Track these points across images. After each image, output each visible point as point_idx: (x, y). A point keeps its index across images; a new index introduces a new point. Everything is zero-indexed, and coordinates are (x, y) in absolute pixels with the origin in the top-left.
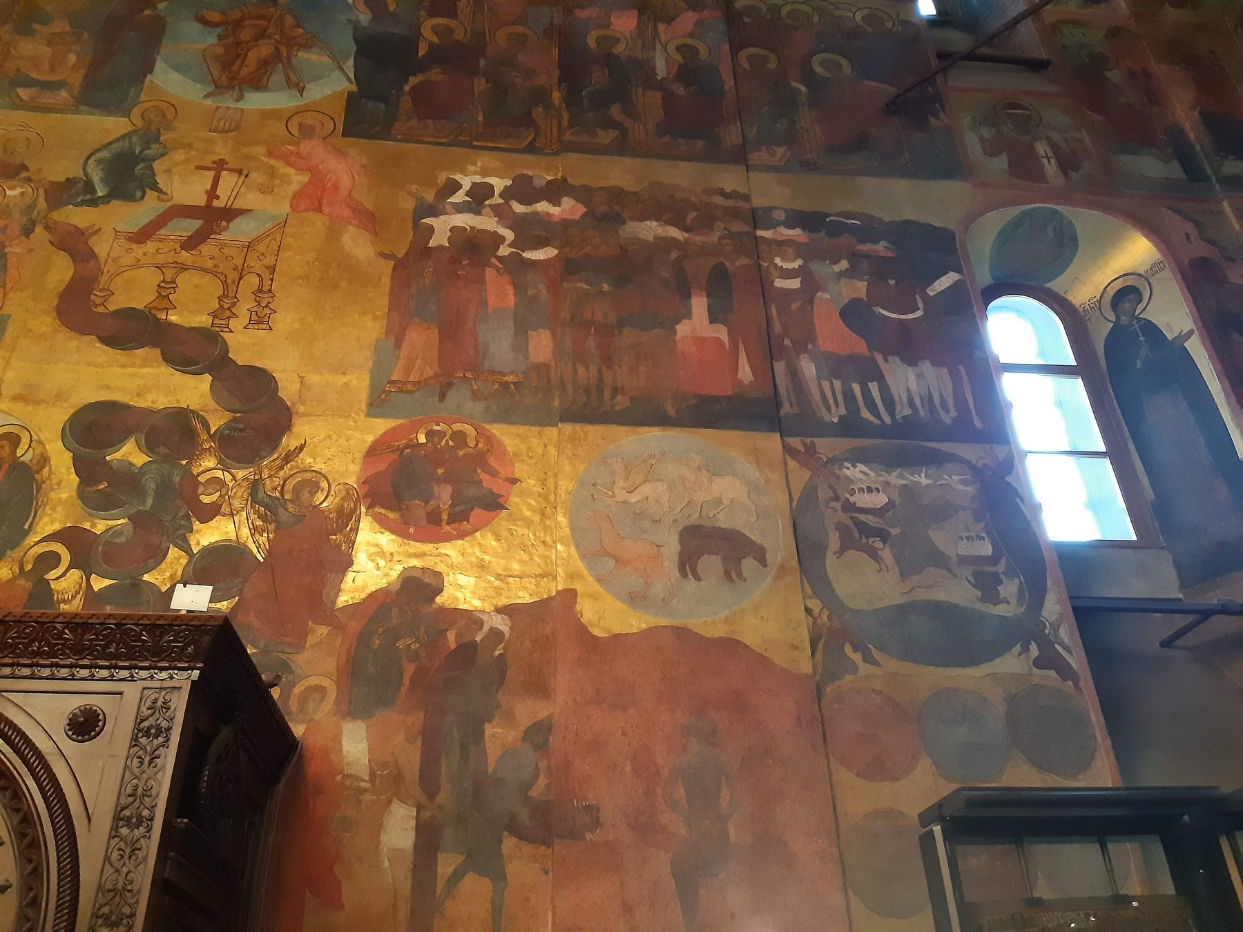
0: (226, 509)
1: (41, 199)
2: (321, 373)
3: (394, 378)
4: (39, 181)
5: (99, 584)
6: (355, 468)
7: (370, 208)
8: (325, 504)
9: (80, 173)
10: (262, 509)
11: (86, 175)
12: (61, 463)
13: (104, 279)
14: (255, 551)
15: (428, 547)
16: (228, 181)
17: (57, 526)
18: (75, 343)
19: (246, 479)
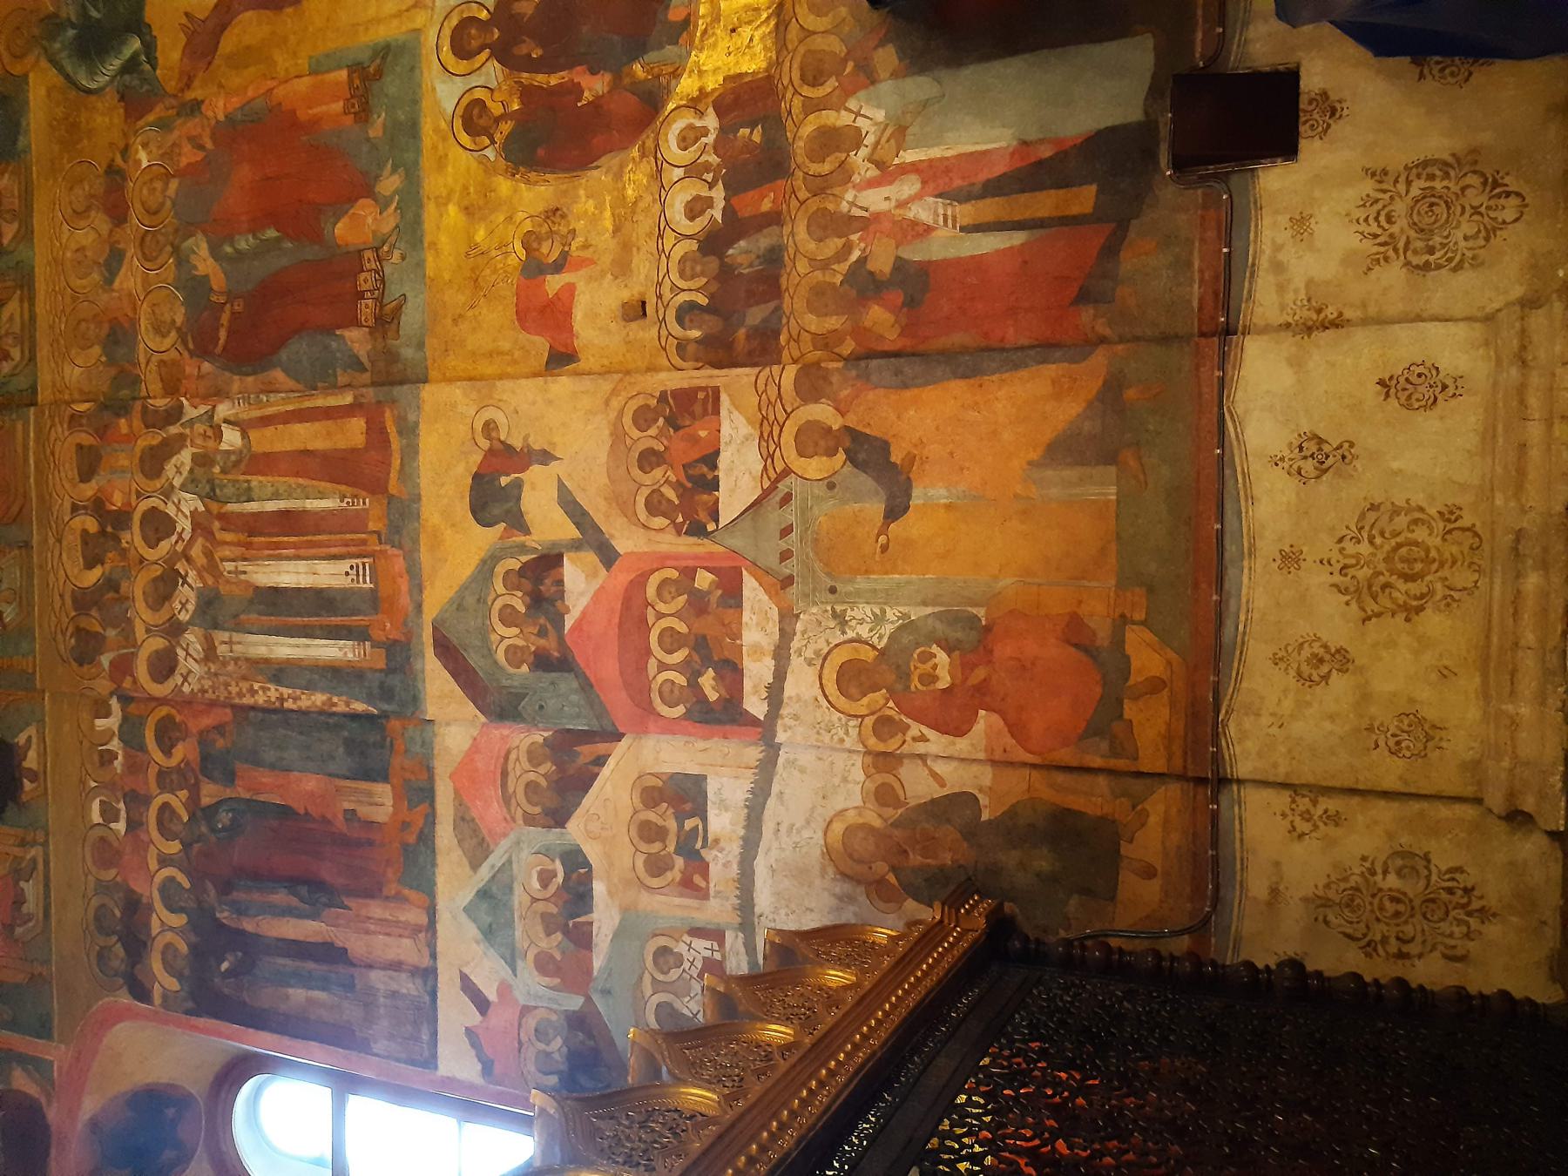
1: (151, 118)
4: (125, 135)
9: (111, 97)
11: (114, 77)
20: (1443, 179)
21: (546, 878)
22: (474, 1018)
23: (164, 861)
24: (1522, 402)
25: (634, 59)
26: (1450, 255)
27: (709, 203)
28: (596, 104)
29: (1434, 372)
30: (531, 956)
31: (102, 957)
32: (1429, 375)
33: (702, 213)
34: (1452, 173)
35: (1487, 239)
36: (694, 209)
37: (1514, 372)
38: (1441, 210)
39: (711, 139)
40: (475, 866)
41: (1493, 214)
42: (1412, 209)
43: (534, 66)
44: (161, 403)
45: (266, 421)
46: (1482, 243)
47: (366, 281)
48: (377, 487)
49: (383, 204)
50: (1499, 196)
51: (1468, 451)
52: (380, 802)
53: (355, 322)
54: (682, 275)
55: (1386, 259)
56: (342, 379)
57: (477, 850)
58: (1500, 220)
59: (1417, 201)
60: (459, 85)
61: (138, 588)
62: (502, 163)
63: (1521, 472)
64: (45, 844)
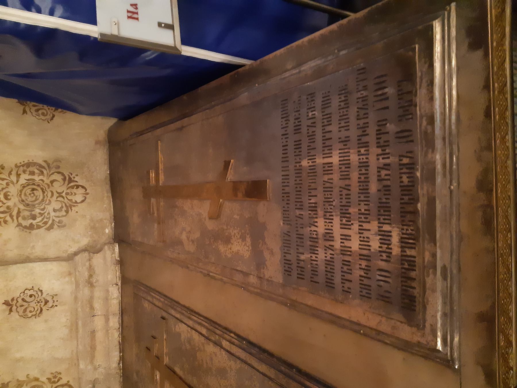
20: (39, 175)
24: (92, 308)
26: (45, 220)
29: (40, 294)
32: (37, 296)
34: (45, 172)
35: (67, 212)
37: (86, 291)
38: (39, 193)
41: (69, 197)
42: (21, 191)
46: (65, 214)
50: (72, 187)
51: (63, 339)
55: (5, 222)
58: (74, 201)
59: (24, 187)
63: (93, 348)
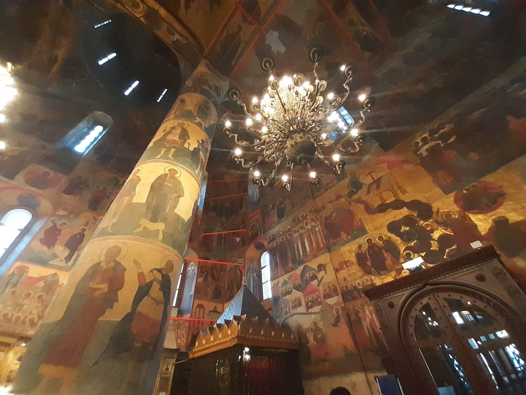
0: (434, 229)
2: (427, 194)
3: (444, 184)
5: (423, 254)
6: (455, 206)
7: (404, 159)
8: (456, 217)
9: (349, 190)
10: (442, 225)
12: (393, 237)
13: (370, 203)
14: (450, 233)
15: (494, 212)
16: (373, 174)
17: (404, 248)
18: (375, 216)
19: (432, 221)
21: (289, 288)
22: (276, 284)
23: (279, 240)
25: (374, 268)
27: (360, 286)
28: (367, 264)
30: (282, 289)
31: (271, 237)
33: (358, 285)
36: (359, 284)
39: (368, 284)
40: (288, 279)
43: (369, 252)
44: (318, 218)
45: (320, 233)
47: (338, 239)
48: (317, 251)
49: (347, 237)
52: (290, 265)
53: (333, 240)
54: (351, 285)
56: (327, 241)
57: (289, 279)
60: (363, 242)
61: (301, 224)
62: (356, 253)
64: (277, 225)
